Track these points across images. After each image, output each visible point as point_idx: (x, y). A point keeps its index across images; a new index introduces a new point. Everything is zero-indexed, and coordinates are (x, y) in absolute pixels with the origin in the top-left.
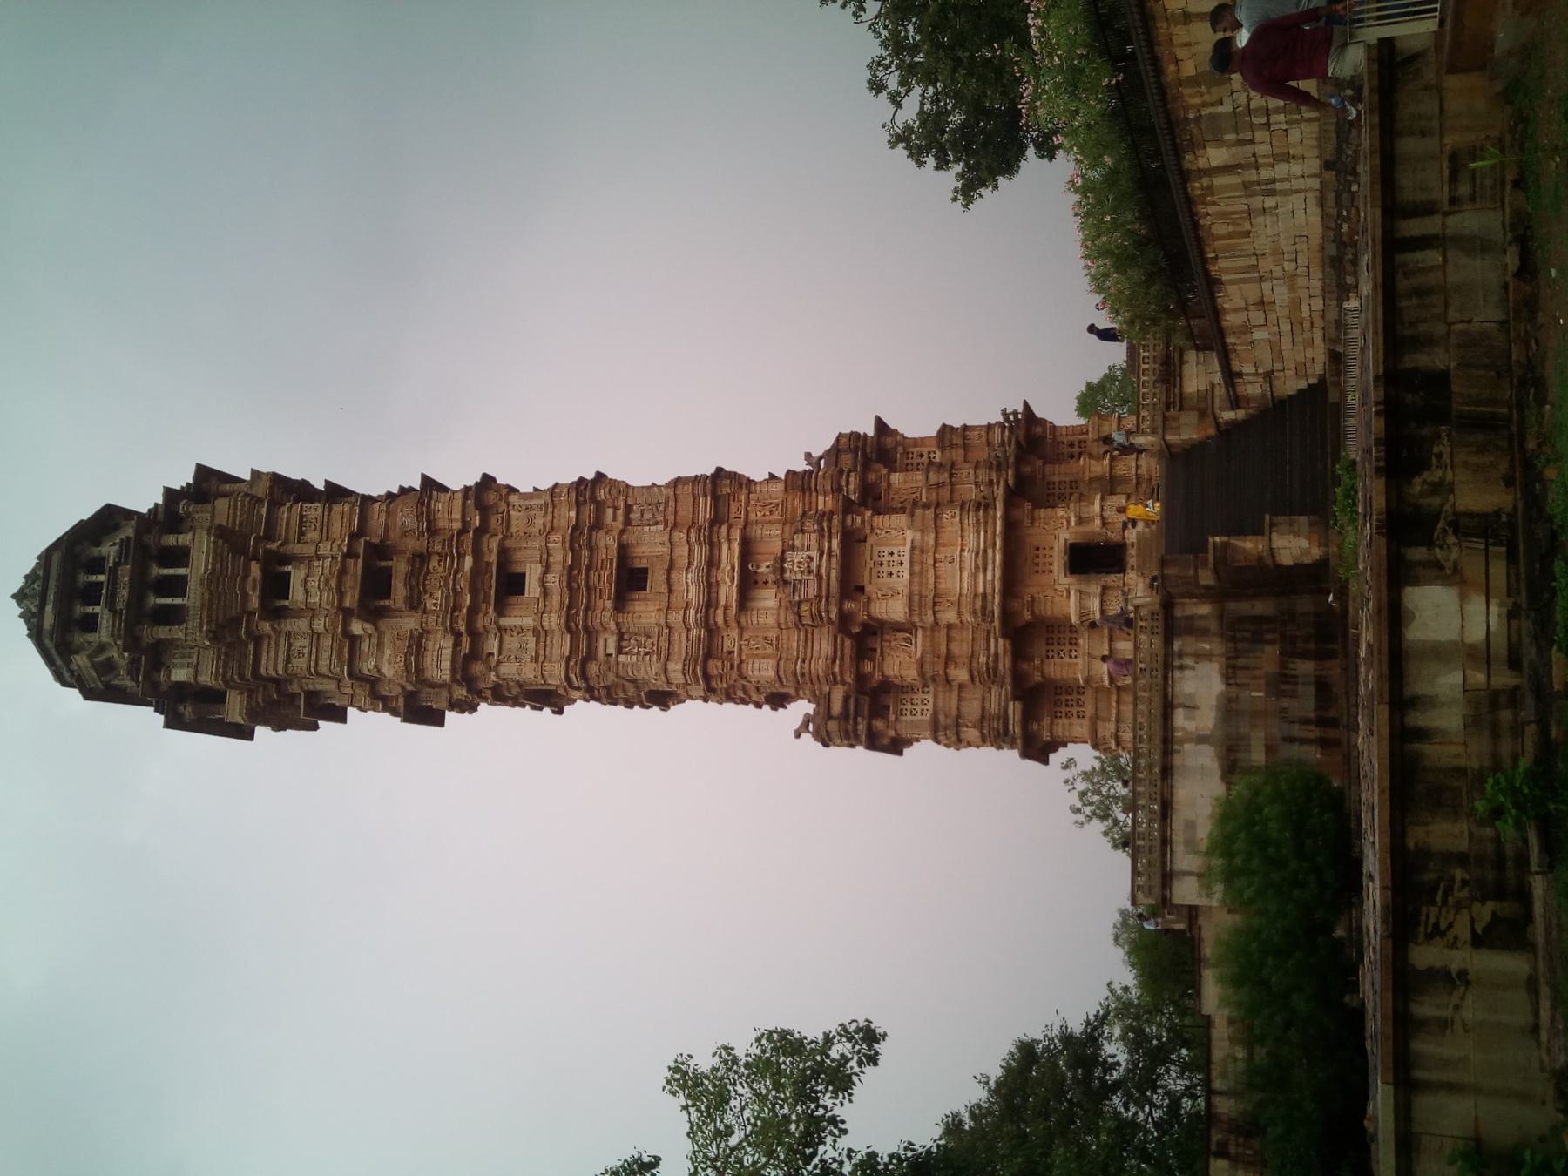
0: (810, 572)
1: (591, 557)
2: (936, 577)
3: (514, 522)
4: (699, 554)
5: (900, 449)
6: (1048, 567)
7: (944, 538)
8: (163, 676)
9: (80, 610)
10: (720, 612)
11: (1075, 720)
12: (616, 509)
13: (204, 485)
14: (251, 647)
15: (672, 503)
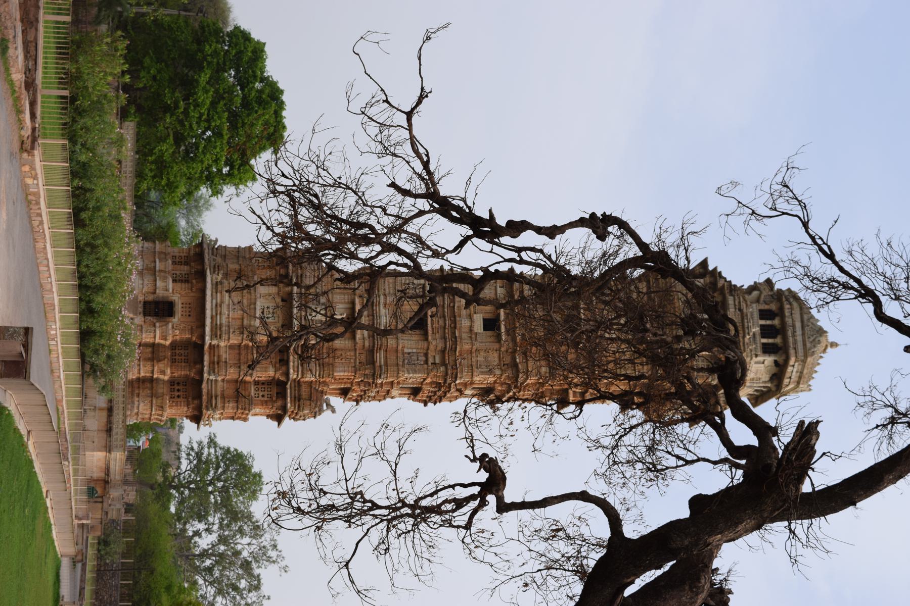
1: (445, 333)
3: (497, 359)
5: (274, 399)
7: (238, 323)
8: (708, 279)
9: (776, 322)
11: (177, 255)
12: (434, 364)
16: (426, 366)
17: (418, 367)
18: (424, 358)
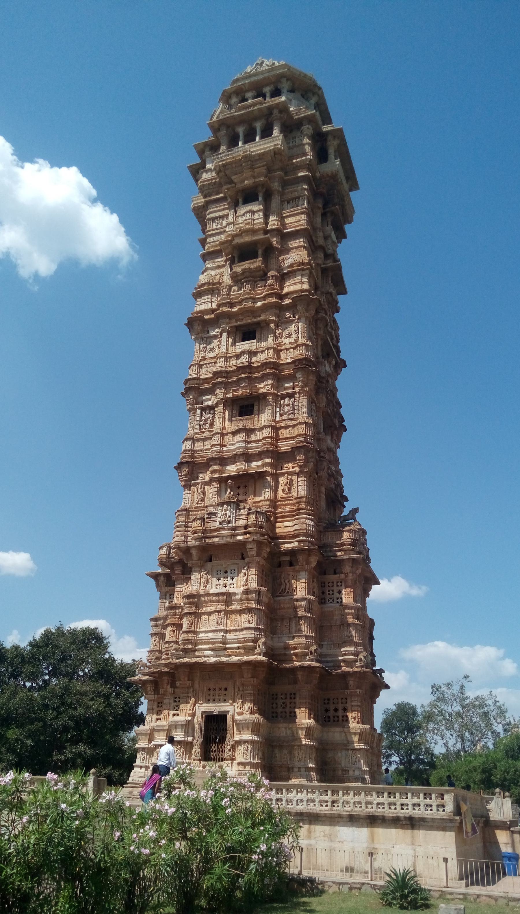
0: (220, 523)
1: (257, 378)
2: (210, 614)
4: (255, 448)
5: (343, 576)
6: (212, 698)
10: (217, 467)
13: (330, 138)
14: (221, 195)
15: (294, 422)
16: (296, 396)
17: (296, 403)
18: (287, 399)
